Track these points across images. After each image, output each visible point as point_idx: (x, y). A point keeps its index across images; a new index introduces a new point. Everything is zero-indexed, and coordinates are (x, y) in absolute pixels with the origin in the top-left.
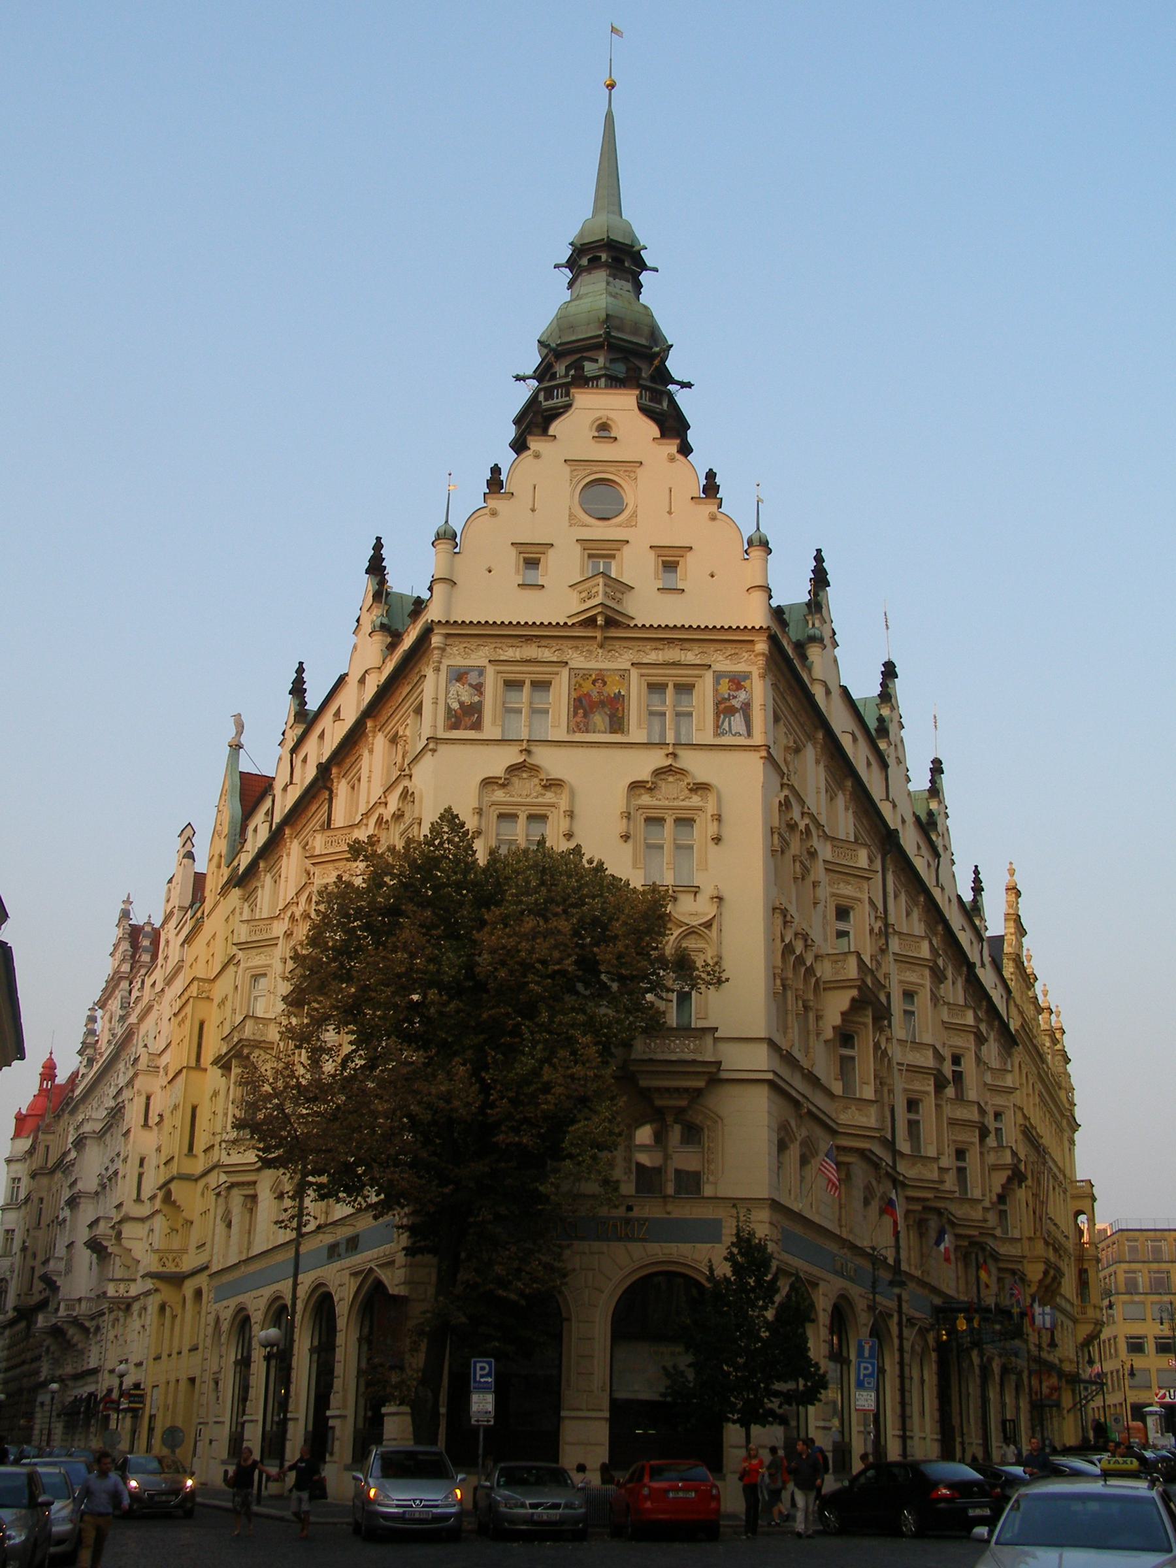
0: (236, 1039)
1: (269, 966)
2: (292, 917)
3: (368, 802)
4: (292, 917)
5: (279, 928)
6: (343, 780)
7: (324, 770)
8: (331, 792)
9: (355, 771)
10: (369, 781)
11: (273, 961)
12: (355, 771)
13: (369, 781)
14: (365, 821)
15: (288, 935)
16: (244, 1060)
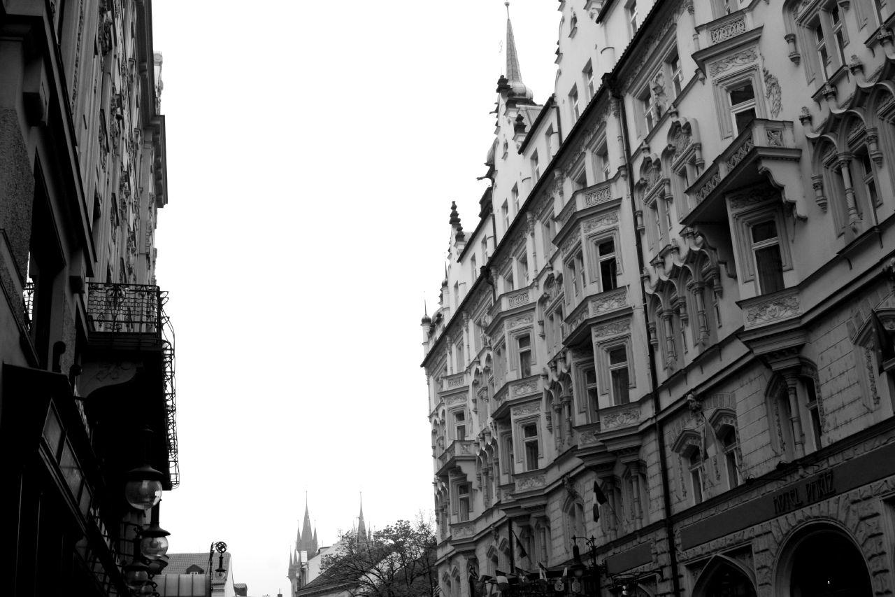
0: (448, 459)
1: (465, 405)
2: (477, 371)
3: (536, 271)
4: (477, 371)
5: (469, 380)
6: (500, 276)
7: (486, 271)
8: (493, 286)
9: (522, 250)
10: (535, 256)
11: (467, 402)
12: (522, 250)
13: (535, 256)
14: (536, 284)
15: (475, 384)
16: (457, 471)
